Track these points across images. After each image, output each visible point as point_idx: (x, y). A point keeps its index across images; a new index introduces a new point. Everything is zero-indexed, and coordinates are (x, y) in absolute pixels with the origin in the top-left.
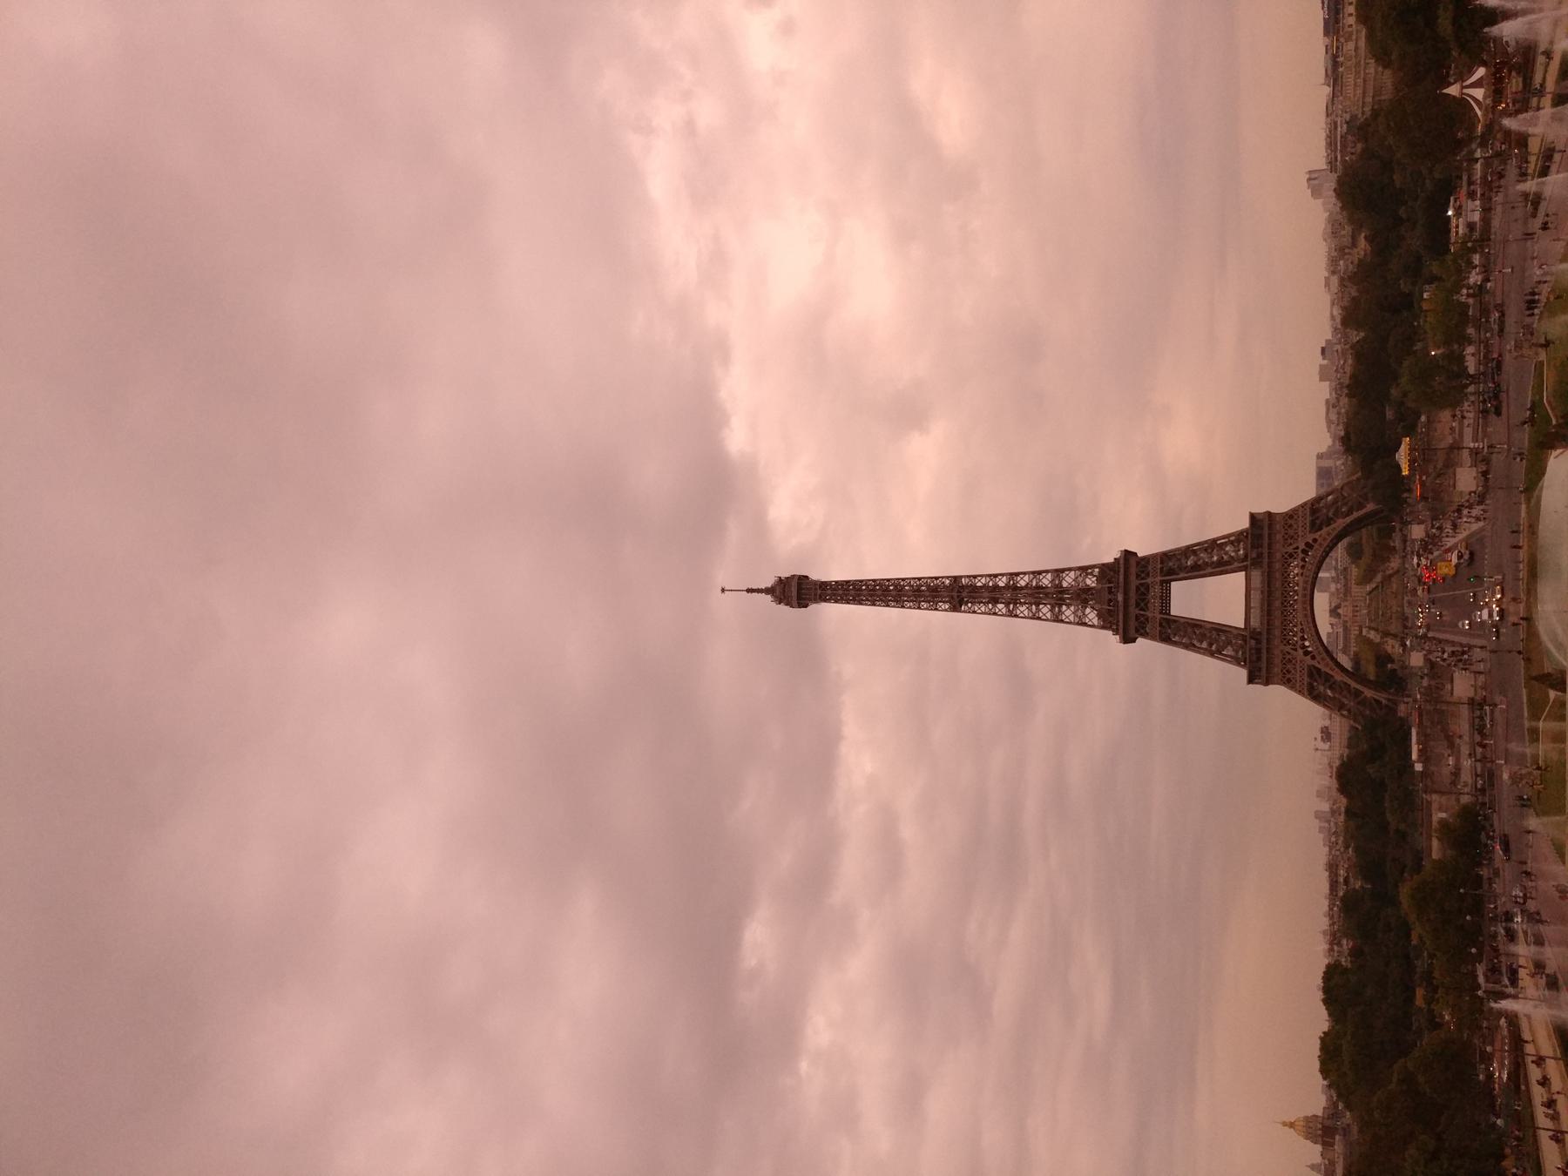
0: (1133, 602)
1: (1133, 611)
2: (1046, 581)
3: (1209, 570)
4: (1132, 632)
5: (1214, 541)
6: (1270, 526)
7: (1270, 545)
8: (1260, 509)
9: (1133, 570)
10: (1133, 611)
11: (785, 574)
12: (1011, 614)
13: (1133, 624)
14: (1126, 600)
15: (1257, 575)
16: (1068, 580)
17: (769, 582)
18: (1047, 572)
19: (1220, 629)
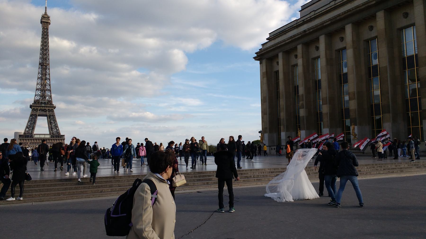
0: (41, 108)
1: (39, 108)
2: (48, 87)
3: (50, 126)
4: (33, 108)
5: (58, 127)
6: (61, 140)
7: (56, 140)
8: (66, 137)
9: (50, 108)
10: (39, 108)
11: (51, 18)
12: (38, 78)
13: (35, 108)
14: (43, 107)
15: (48, 136)
16: (48, 93)
17: (49, 13)
18: (50, 88)
19: (33, 128)
